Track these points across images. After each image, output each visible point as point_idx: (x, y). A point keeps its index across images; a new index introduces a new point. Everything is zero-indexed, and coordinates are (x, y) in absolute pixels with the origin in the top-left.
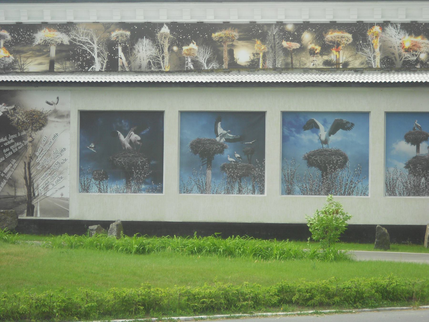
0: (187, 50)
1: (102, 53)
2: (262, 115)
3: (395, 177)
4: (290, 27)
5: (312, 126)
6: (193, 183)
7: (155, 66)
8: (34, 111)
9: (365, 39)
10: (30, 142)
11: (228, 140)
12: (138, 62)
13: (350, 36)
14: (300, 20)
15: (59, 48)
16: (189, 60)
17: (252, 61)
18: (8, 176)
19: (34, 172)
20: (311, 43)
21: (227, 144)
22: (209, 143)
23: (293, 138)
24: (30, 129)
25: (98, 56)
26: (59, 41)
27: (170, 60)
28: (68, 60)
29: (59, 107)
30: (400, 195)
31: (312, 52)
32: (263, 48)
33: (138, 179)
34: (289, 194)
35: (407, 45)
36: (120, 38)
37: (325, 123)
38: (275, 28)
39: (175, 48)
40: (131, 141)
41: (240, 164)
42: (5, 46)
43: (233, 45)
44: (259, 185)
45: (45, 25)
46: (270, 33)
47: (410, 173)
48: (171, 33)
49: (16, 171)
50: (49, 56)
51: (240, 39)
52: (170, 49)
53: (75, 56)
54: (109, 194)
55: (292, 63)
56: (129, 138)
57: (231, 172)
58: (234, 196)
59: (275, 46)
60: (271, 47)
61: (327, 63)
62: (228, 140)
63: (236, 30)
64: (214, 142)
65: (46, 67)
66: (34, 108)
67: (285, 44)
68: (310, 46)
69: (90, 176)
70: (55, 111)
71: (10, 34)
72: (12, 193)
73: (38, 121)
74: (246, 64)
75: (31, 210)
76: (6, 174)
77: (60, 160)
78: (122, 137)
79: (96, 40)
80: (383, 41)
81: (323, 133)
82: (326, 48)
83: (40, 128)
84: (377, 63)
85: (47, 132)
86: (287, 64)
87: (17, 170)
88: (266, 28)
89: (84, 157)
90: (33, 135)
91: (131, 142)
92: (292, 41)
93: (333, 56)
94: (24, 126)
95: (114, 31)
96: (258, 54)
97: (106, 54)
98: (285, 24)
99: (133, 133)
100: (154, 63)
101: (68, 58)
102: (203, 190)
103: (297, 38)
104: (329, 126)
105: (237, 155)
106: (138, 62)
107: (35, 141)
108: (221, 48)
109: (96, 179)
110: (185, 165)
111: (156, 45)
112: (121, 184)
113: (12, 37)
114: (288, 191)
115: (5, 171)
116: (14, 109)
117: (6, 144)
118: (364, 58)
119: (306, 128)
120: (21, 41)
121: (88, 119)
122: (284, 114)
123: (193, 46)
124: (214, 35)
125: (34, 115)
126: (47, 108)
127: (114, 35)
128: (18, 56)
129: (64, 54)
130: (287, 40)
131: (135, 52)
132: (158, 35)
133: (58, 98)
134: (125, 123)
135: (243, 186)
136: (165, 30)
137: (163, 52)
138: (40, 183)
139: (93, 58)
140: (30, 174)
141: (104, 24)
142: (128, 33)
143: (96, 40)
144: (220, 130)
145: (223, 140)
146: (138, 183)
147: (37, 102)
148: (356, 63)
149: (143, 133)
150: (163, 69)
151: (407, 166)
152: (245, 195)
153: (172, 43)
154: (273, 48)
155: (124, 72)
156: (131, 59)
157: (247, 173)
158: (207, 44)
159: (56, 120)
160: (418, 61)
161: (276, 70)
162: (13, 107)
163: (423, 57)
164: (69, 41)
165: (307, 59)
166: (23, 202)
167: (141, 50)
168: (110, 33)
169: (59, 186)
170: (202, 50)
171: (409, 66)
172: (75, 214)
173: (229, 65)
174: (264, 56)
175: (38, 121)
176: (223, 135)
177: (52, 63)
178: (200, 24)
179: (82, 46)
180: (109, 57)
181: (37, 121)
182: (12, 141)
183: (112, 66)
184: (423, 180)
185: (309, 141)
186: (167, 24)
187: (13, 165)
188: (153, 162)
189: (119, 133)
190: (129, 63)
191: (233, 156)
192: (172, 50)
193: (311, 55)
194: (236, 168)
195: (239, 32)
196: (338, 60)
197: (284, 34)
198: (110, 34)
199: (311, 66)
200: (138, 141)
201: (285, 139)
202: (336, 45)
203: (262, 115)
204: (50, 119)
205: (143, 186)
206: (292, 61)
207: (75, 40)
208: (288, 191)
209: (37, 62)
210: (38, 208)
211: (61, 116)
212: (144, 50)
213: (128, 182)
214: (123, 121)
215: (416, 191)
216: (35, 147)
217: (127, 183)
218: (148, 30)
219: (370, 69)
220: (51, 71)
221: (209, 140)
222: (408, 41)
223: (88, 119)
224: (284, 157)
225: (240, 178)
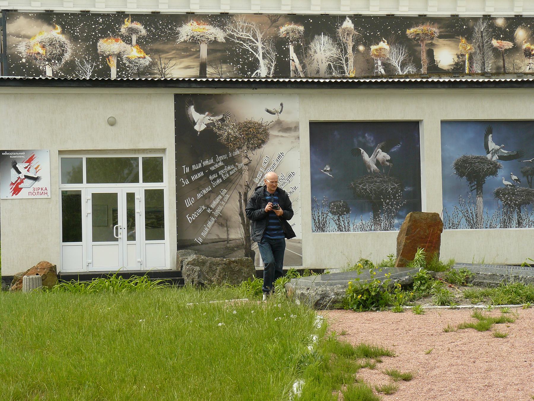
0: (376, 50)
1: (269, 53)
4: (500, 22)
6: (461, 215)
8: (250, 123)
10: (246, 165)
11: (501, 158)
12: (315, 65)
14: (512, 13)
15: (211, 47)
16: (380, 63)
17: (457, 64)
18: (217, 213)
20: (526, 42)
21: (501, 163)
22: (479, 162)
24: (245, 148)
25: (264, 57)
27: (355, 63)
28: (225, 62)
29: (283, 117)
32: (469, 48)
33: (389, 212)
36: (291, 34)
38: (483, 23)
39: (361, 48)
40: (377, 161)
41: (519, 188)
42: (137, 43)
43: (432, 45)
45: (190, 16)
46: (477, 29)
48: (356, 28)
49: (229, 205)
50: (198, 57)
51: (440, 37)
52: (355, 49)
54: (352, 232)
55: (504, 66)
56: (375, 158)
57: (507, 199)
58: (513, 230)
59: (483, 46)
60: (479, 47)
62: (501, 158)
63: (436, 25)
64: (484, 160)
66: (249, 119)
68: (525, 46)
69: (326, 210)
71: (145, 28)
72: (224, 236)
73: (255, 135)
74: (449, 68)
76: (214, 210)
78: (366, 156)
79: (260, 37)
83: (259, 146)
85: (269, 150)
86: (498, 68)
88: (471, 23)
90: (250, 155)
91: (378, 163)
92: (503, 39)
94: (236, 143)
95: (283, 25)
96: (463, 55)
97: (274, 54)
98: (494, 19)
99: (380, 150)
100: (335, 67)
102: (473, 224)
103: (510, 36)
106: (315, 65)
107: (252, 163)
108: (418, 48)
109: (333, 213)
111: (338, 44)
112: (367, 219)
113: (147, 31)
115: (213, 206)
116: (222, 120)
117: (213, 168)
120: (160, 36)
123: (383, 45)
124: (408, 32)
125: (250, 128)
126: (267, 119)
127: (283, 30)
128: (156, 56)
129: (219, 54)
130: (498, 38)
131: (311, 52)
132: (340, 30)
133: (282, 105)
134: (369, 137)
135: (524, 217)
136: (348, 24)
137: (346, 53)
139: (257, 60)
141: (269, 16)
142: (301, 28)
143: (260, 37)
144: (492, 146)
146: (390, 218)
149: (393, 150)
150: (347, 74)
152: (527, 228)
153: (357, 42)
154: (481, 48)
156: (306, 61)
158: (401, 43)
159: (281, 134)
161: (483, 74)
162: (221, 117)
164: (225, 38)
165: (522, 61)
166: (238, 247)
167: (318, 51)
168: (278, 27)
170: (395, 50)
173: (428, 69)
174: (471, 58)
175: (255, 135)
176: (496, 152)
178: (390, 17)
179: (242, 45)
180: (278, 59)
181: (255, 136)
182: (221, 164)
186: (350, 17)
187: (223, 197)
188: (407, 189)
189: (362, 150)
190: (304, 67)
191: (508, 178)
192: (358, 51)
193: (526, 56)
194: (513, 194)
195: (439, 28)
197: (494, 31)
198: (279, 30)
199: (527, 71)
200: (387, 161)
204: (272, 132)
205: (396, 221)
206: (504, 64)
207: (232, 36)
209: (182, 65)
211: (287, 129)
212: (323, 50)
213: (376, 216)
214: (366, 135)
217: (374, 217)
221: (478, 158)
225: (519, 206)
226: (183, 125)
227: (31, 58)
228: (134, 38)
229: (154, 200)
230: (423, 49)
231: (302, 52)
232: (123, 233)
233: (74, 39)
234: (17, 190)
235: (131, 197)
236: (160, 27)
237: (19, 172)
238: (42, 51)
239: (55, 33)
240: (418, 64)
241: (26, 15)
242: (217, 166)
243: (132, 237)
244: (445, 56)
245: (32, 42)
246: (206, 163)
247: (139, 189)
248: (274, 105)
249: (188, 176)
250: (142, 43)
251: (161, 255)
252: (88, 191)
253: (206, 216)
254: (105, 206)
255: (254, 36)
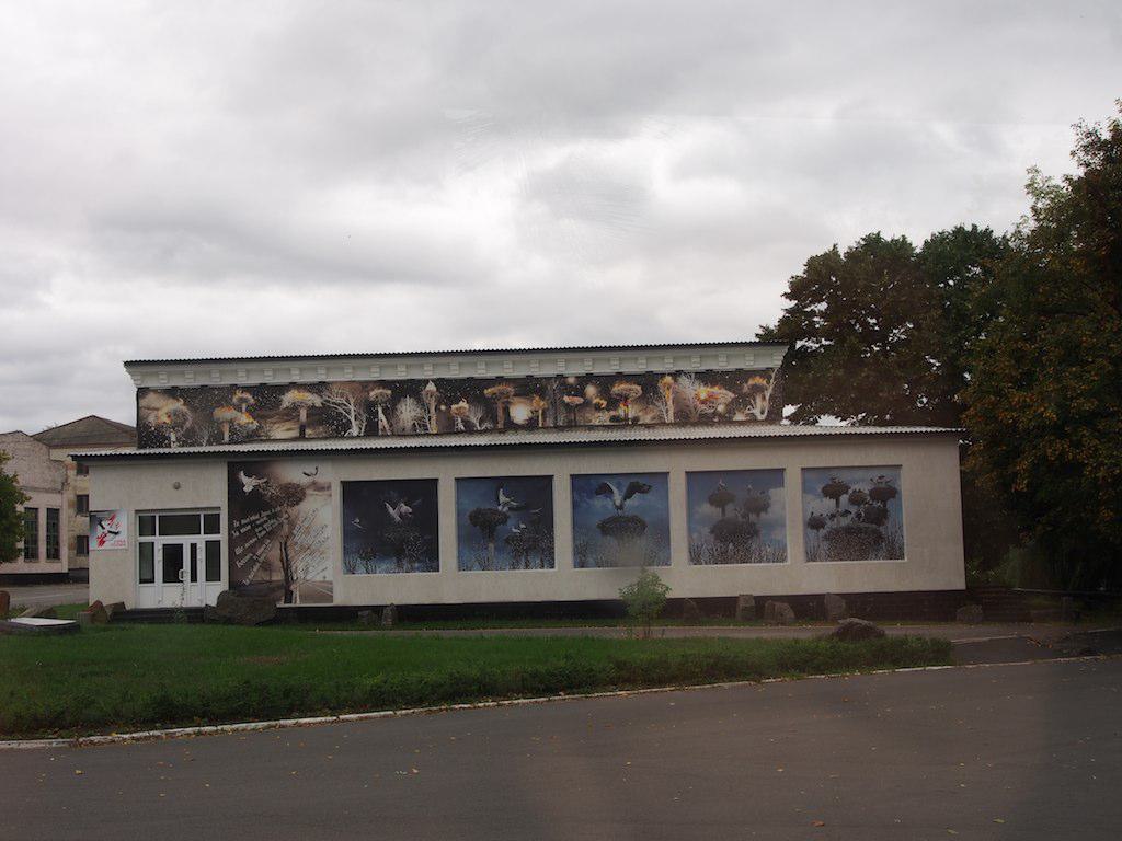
2: (548, 480)
3: (894, 531)
4: (571, 380)
5: (605, 490)
7: (419, 428)
9: (656, 391)
13: (639, 388)
16: (460, 420)
17: (531, 419)
18: (262, 559)
19: (291, 553)
23: (585, 504)
26: (310, 403)
28: (321, 424)
30: (706, 563)
31: (598, 408)
33: (411, 556)
34: (582, 567)
35: (703, 396)
36: (380, 398)
37: (619, 486)
39: (443, 408)
43: (508, 402)
44: (548, 559)
45: (293, 385)
47: (716, 539)
51: (515, 395)
53: (328, 419)
56: (399, 511)
61: (614, 419)
65: (295, 433)
67: (567, 399)
68: (595, 401)
70: (314, 483)
75: (289, 597)
77: (321, 538)
78: (391, 510)
79: (352, 401)
80: (676, 393)
81: (618, 498)
82: (613, 403)
83: (297, 504)
84: (670, 418)
87: (273, 552)
89: (348, 534)
90: (290, 510)
91: (401, 516)
93: (621, 411)
94: (278, 501)
101: (321, 423)
103: (581, 392)
104: (625, 489)
105: (523, 526)
110: (464, 539)
114: (581, 564)
115: (258, 553)
117: (258, 523)
118: (656, 412)
119: (598, 494)
121: (351, 490)
122: (573, 477)
123: (463, 404)
124: (486, 392)
126: (305, 480)
129: (317, 417)
136: (431, 387)
138: (299, 566)
140: (287, 556)
141: (360, 382)
142: (389, 392)
143: (352, 401)
144: (502, 498)
145: (506, 509)
147: (294, 474)
148: (647, 419)
150: (430, 431)
151: (712, 532)
153: (439, 402)
154: (553, 404)
155: (385, 436)
157: (535, 547)
160: (715, 413)
161: (558, 428)
162: (265, 480)
163: (721, 408)
169: (321, 568)
171: (705, 420)
172: (340, 598)
173: (504, 424)
175: (295, 494)
176: (505, 504)
177: (302, 429)
182: (265, 519)
183: (372, 430)
184: (731, 546)
185: (602, 506)
191: (517, 527)
196: (626, 415)
199: (597, 423)
201: (575, 505)
202: (624, 398)
203: (548, 480)
204: (309, 492)
205: (417, 565)
208: (581, 563)
210: (297, 594)
211: (321, 489)
212: (408, 411)
213: (399, 560)
215: (723, 558)
216: (292, 525)
218: (411, 388)
219: (663, 424)
220: (302, 437)
222: (703, 391)
223: (348, 488)
224: (576, 525)
226: (234, 487)
227: (159, 427)
228: (244, 406)
229: (213, 547)
230: (500, 406)
231: (390, 412)
232: (187, 577)
233: (194, 409)
234: (102, 542)
235: (194, 547)
236: (266, 399)
237: (103, 528)
238: (168, 421)
239: (179, 405)
240: (495, 420)
241: (155, 391)
242: (262, 520)
243: (194, 578)
244: (520, 413)
245: (160, 413)
246: (253, 518)
247: (201, 540)
248: (310, 469)
249: (238, 529)
250: (250, 411)
251: (204, 593)
252: (160, 541)
253: (252, 562)
254: (173, 555)
255: (347, 400)
